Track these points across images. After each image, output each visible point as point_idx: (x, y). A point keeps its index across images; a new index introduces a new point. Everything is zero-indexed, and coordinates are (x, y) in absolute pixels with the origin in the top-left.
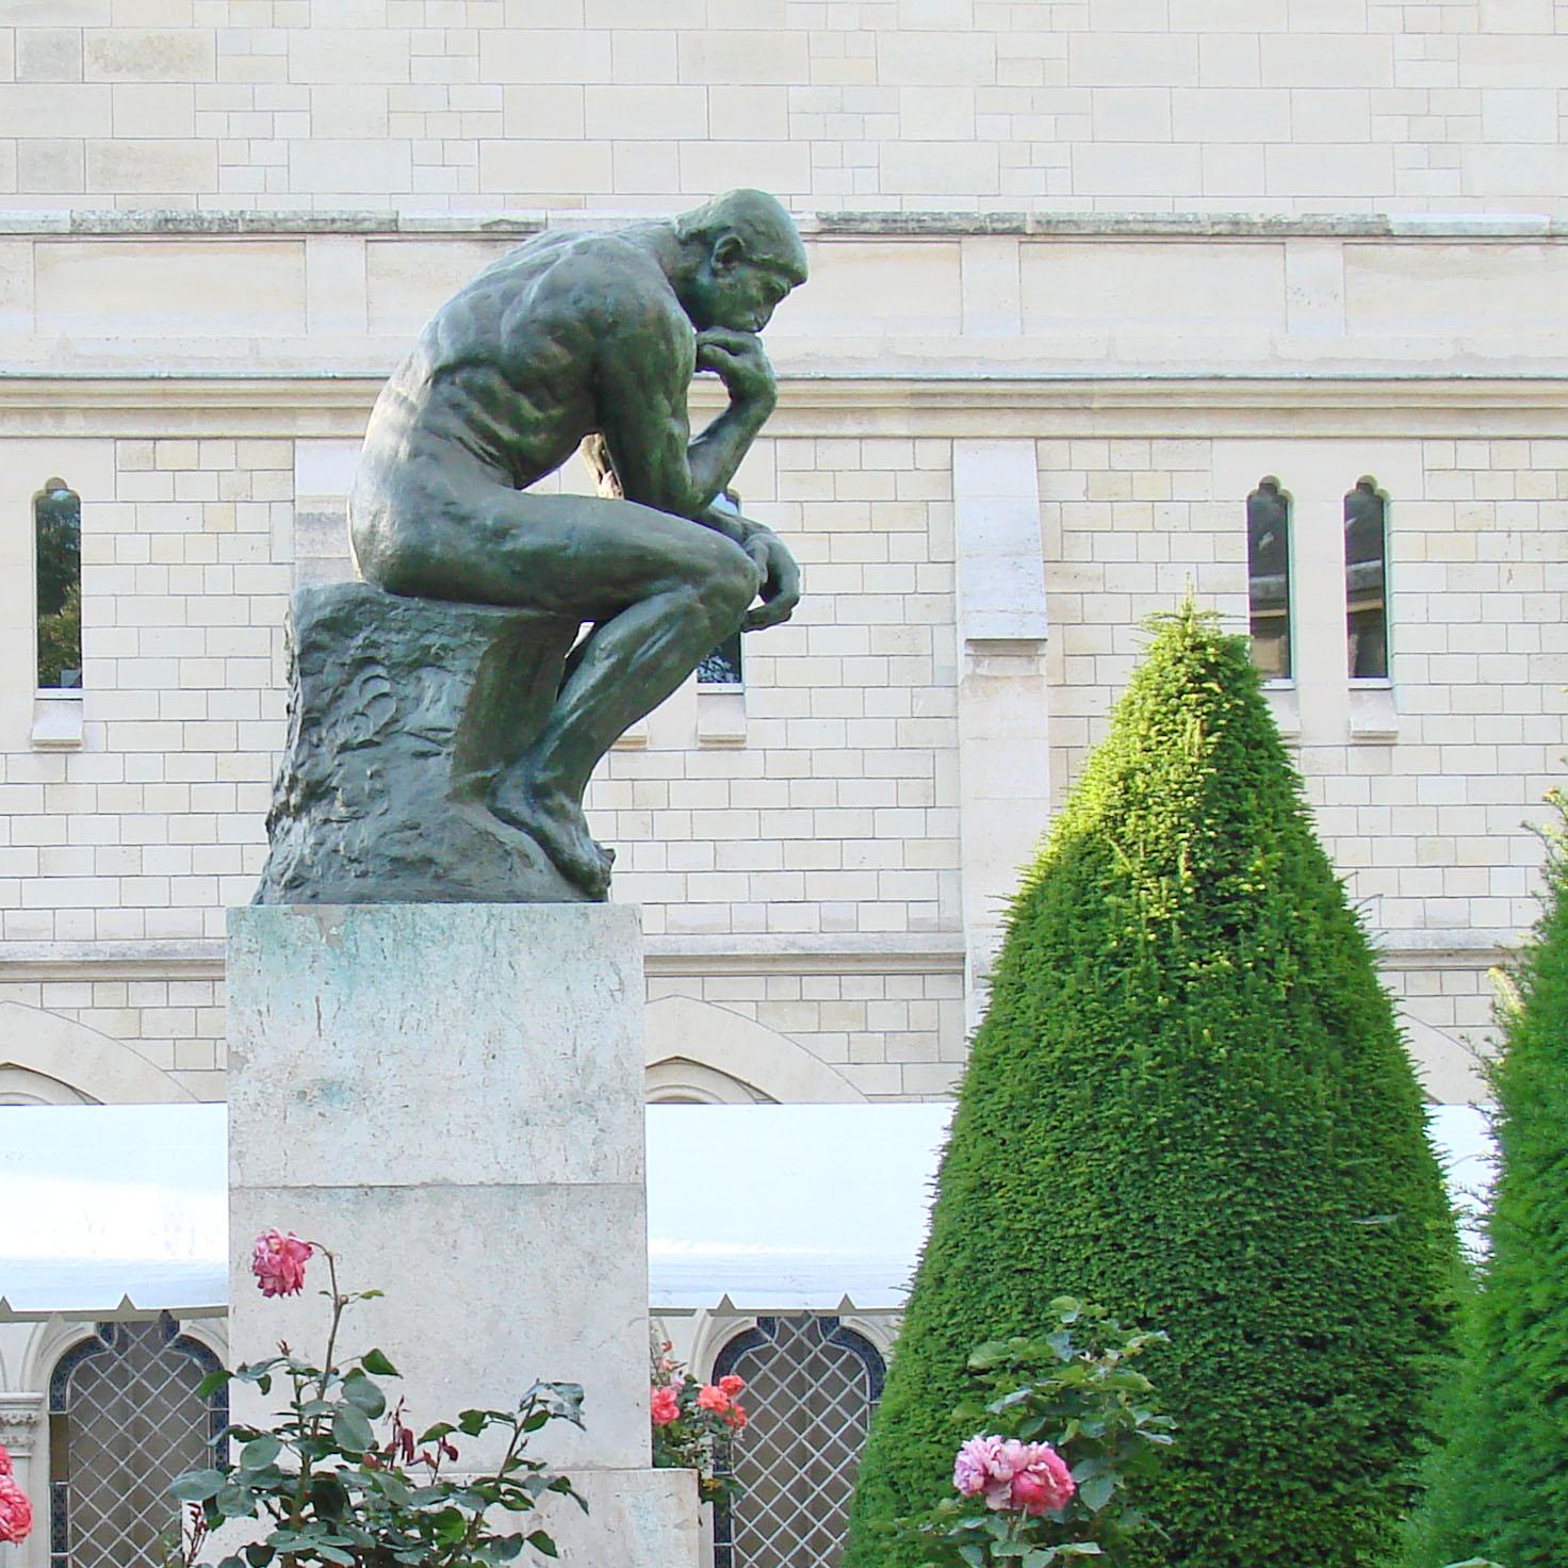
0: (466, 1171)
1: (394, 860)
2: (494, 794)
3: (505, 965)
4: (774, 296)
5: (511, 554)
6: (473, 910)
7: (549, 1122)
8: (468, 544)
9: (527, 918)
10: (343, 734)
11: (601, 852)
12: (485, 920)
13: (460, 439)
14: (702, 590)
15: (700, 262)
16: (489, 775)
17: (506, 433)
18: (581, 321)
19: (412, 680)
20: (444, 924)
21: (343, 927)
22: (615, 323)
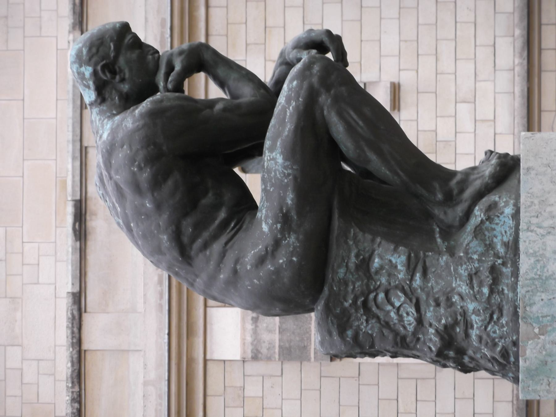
1: (492, 291)
2: (450, 227)
4: (137, 43)
5: (300, 214)
6: (525, 241)
8: (292, 239)
9: (530, 206)
10: (410, 320)
11: (488, 159)
12: (530, 233)
13: (226, 244)
14: (323, 90)
15: (116, 89)
16: (438, 229)
17: (222, 215)
19: (376, 277)
20: (533, 260)
21: (534, 325)
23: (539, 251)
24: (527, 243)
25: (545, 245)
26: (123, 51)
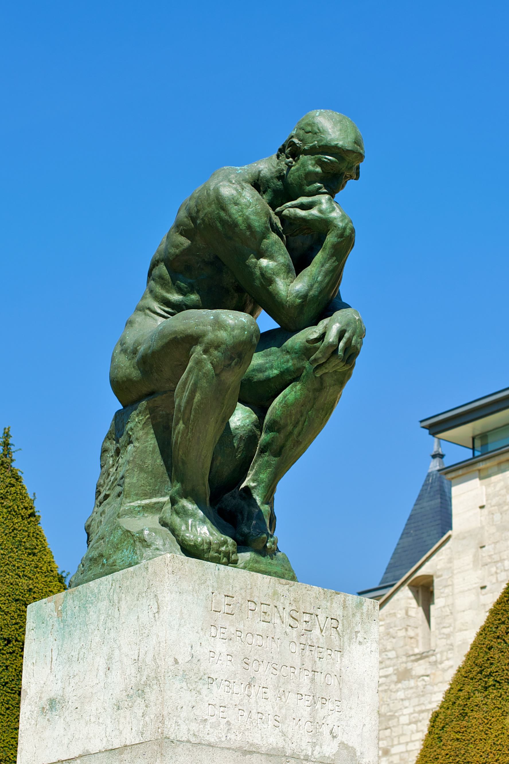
0: (96, 746)
3: (117, 609)
7: (126, 706)
18: (187, 217)
22: (198, 211)
23: (101, 595)
24: (106, 583)
25: (104, 600)
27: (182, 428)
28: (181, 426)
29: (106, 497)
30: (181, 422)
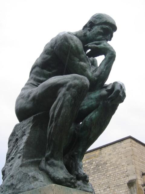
14: (67, 87)
22: (56, 43)
26: (100, 26)
27: (54, 125)
28: (53, 124)
29: (12, 158)
30: (54, 123)
